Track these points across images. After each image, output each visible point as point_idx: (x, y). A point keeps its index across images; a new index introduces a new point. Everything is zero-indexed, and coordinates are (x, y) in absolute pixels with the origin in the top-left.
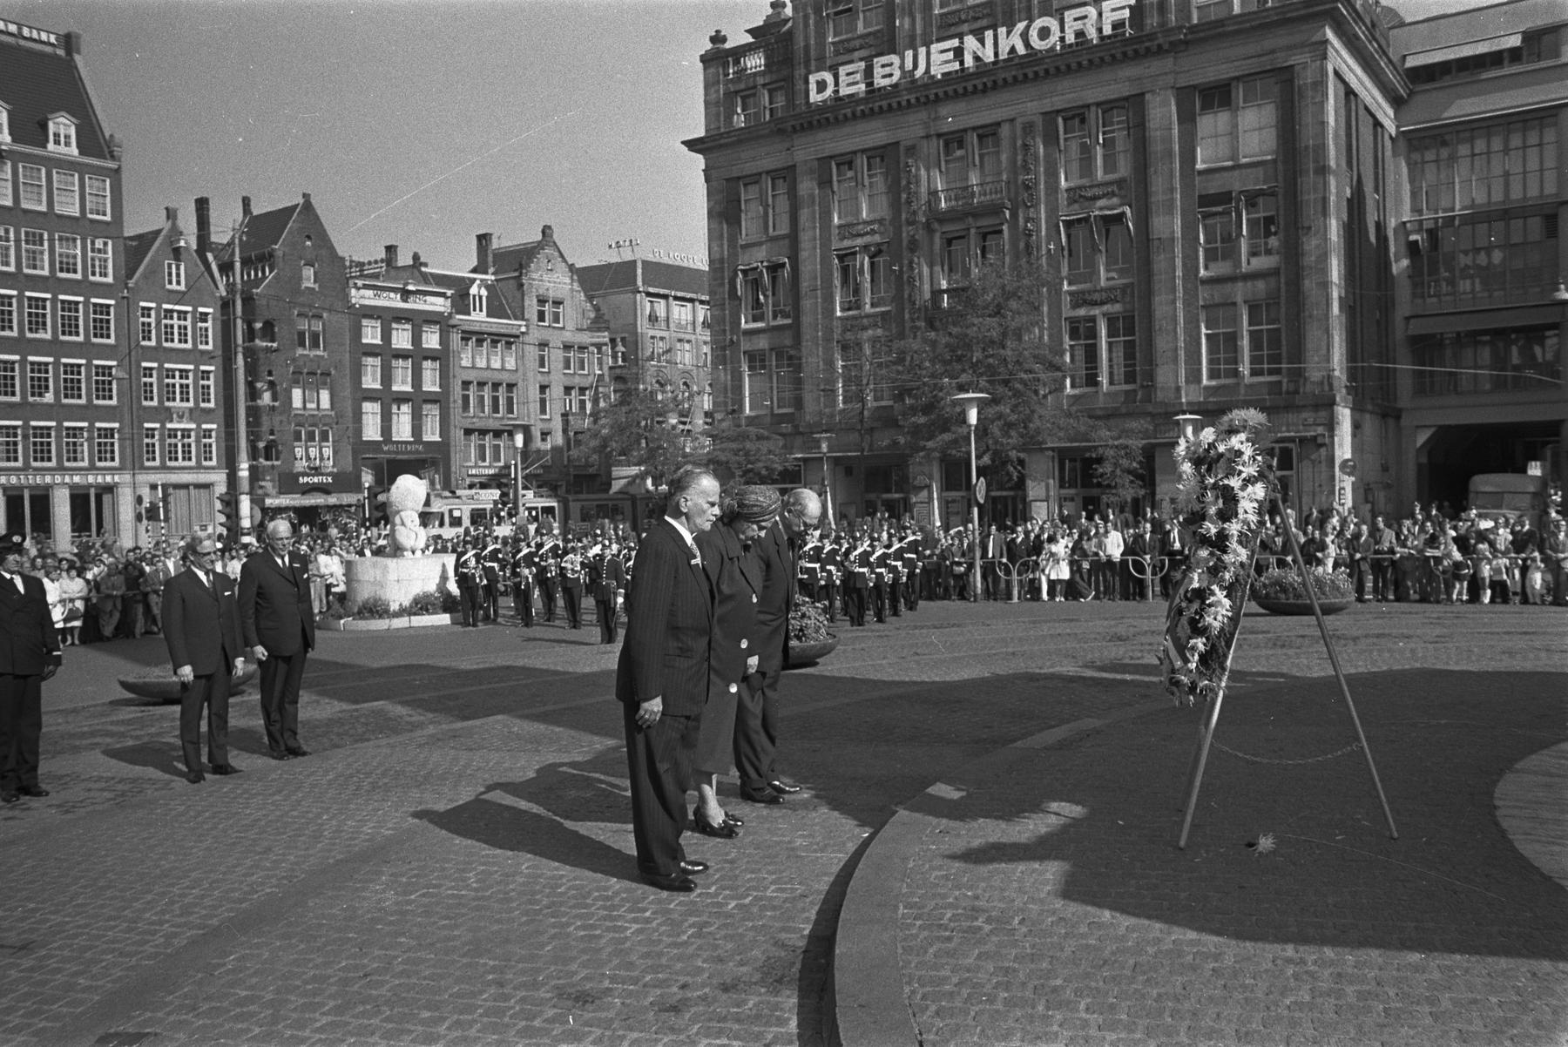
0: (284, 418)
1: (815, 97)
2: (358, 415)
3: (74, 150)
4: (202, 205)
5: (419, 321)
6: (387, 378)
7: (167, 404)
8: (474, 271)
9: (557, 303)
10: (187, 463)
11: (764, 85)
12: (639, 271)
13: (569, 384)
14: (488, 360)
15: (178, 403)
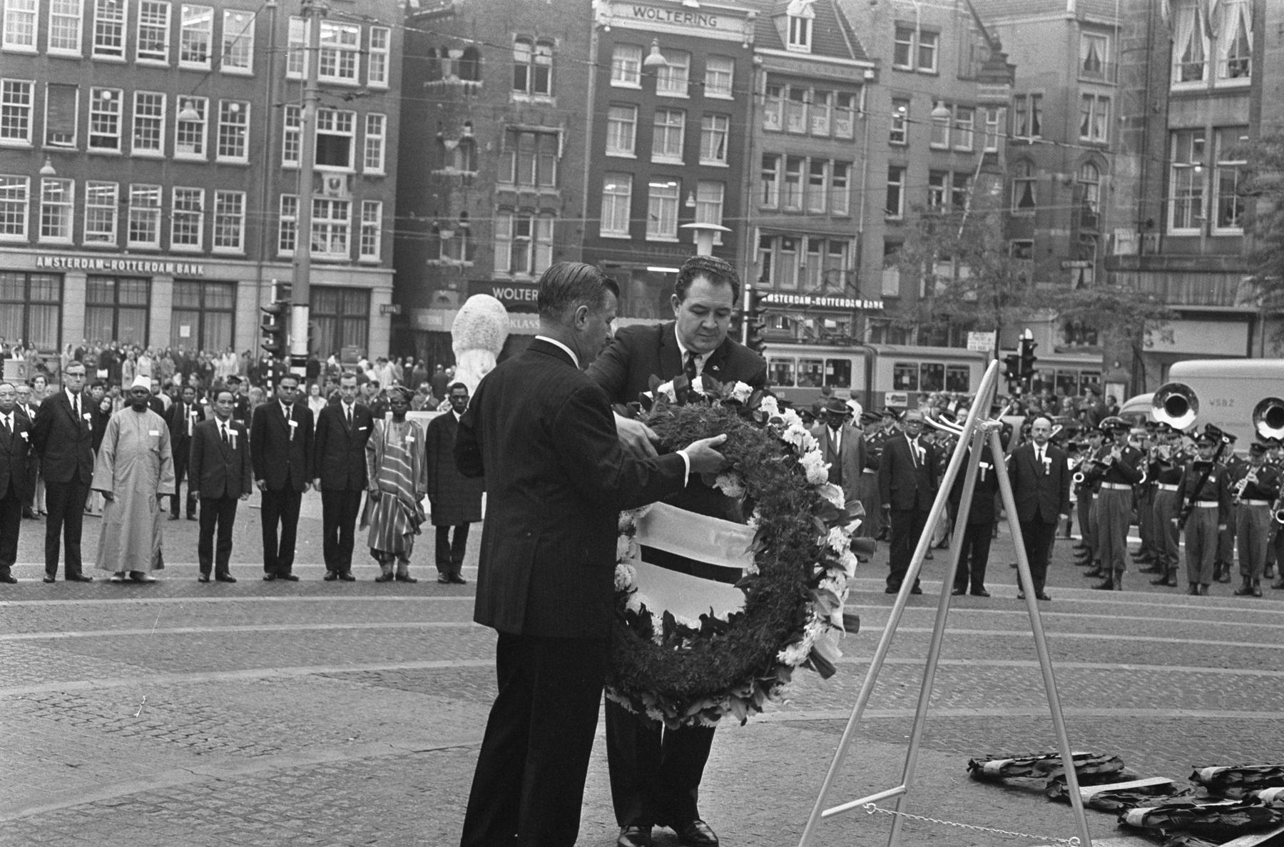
0: (484, 195)
2: (596, 198)
5: (695, 53)
6: (644, 145)
9: (928, 35)
13: (939, 163)
14: (810, 123)
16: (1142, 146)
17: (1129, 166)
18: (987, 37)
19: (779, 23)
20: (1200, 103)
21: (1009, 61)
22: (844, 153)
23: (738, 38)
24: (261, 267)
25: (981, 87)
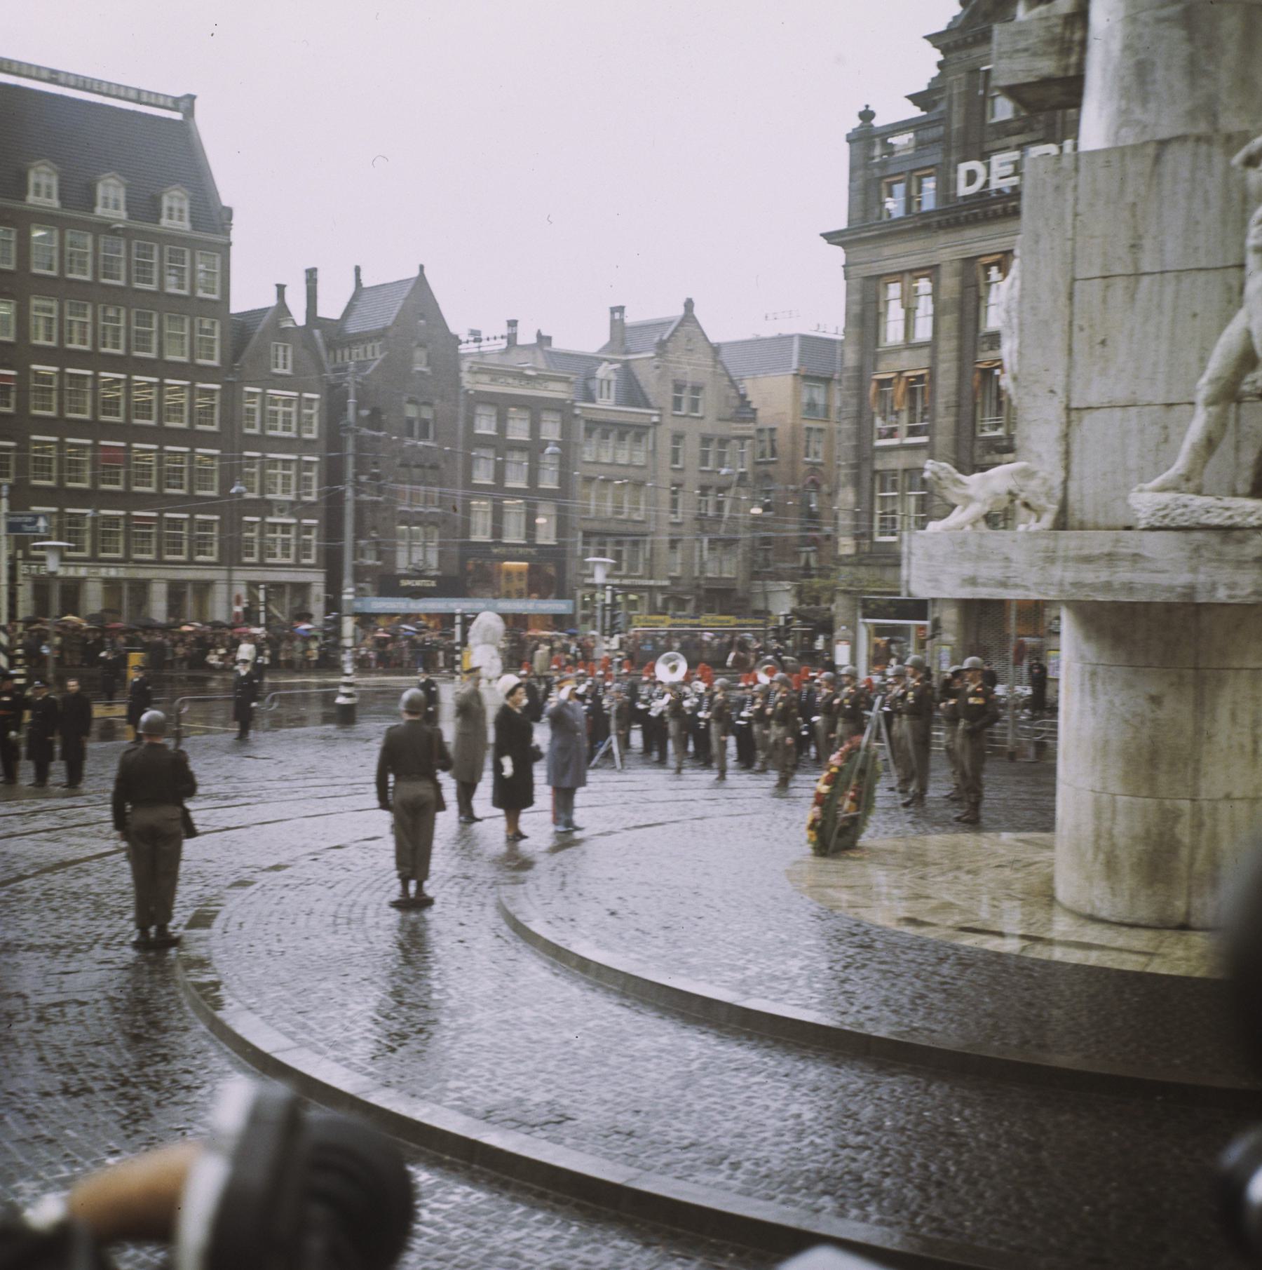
1: (963, 190)
3: (186, 225)
4: (311, 275)
5: (536, 408)
6: (500, 474)
7: (269, 496)
9: (697, 389)
11: (912, 171)
13: (706, 480)
15: (278, 496)
16: (857, 482)
17: (847, 496)
18: (737, 389)
19: (592, 384)
20: (894, 454)
21: (754, 406)
24: (230, 571)
25: (734, 425)
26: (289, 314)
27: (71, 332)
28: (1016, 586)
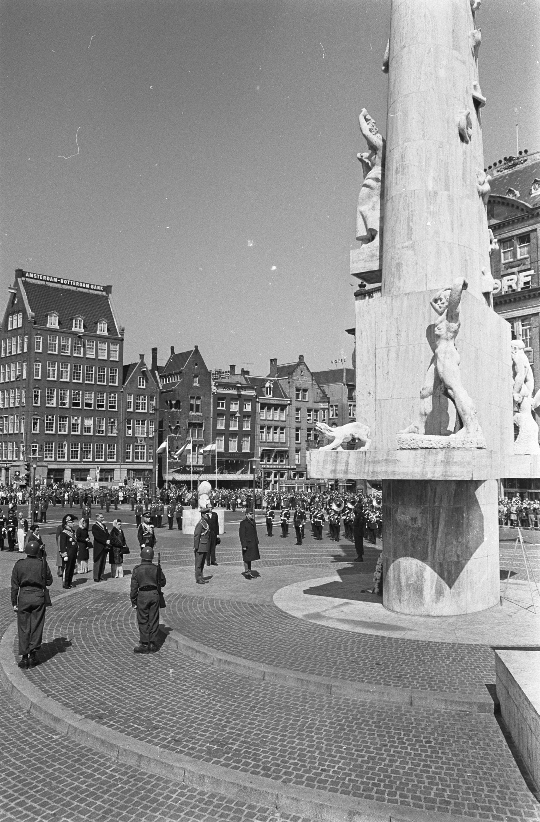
4: (155, 350)
7: (136, 436)
8: (269, 376)
9: (305, 390)
10: (142, 461)
12: (344, 374)
13: (309, 427)
22: (282, 424)
23: (253, 394)
26: (145, 365)
27: (62, 375)
28: (351, 473)
